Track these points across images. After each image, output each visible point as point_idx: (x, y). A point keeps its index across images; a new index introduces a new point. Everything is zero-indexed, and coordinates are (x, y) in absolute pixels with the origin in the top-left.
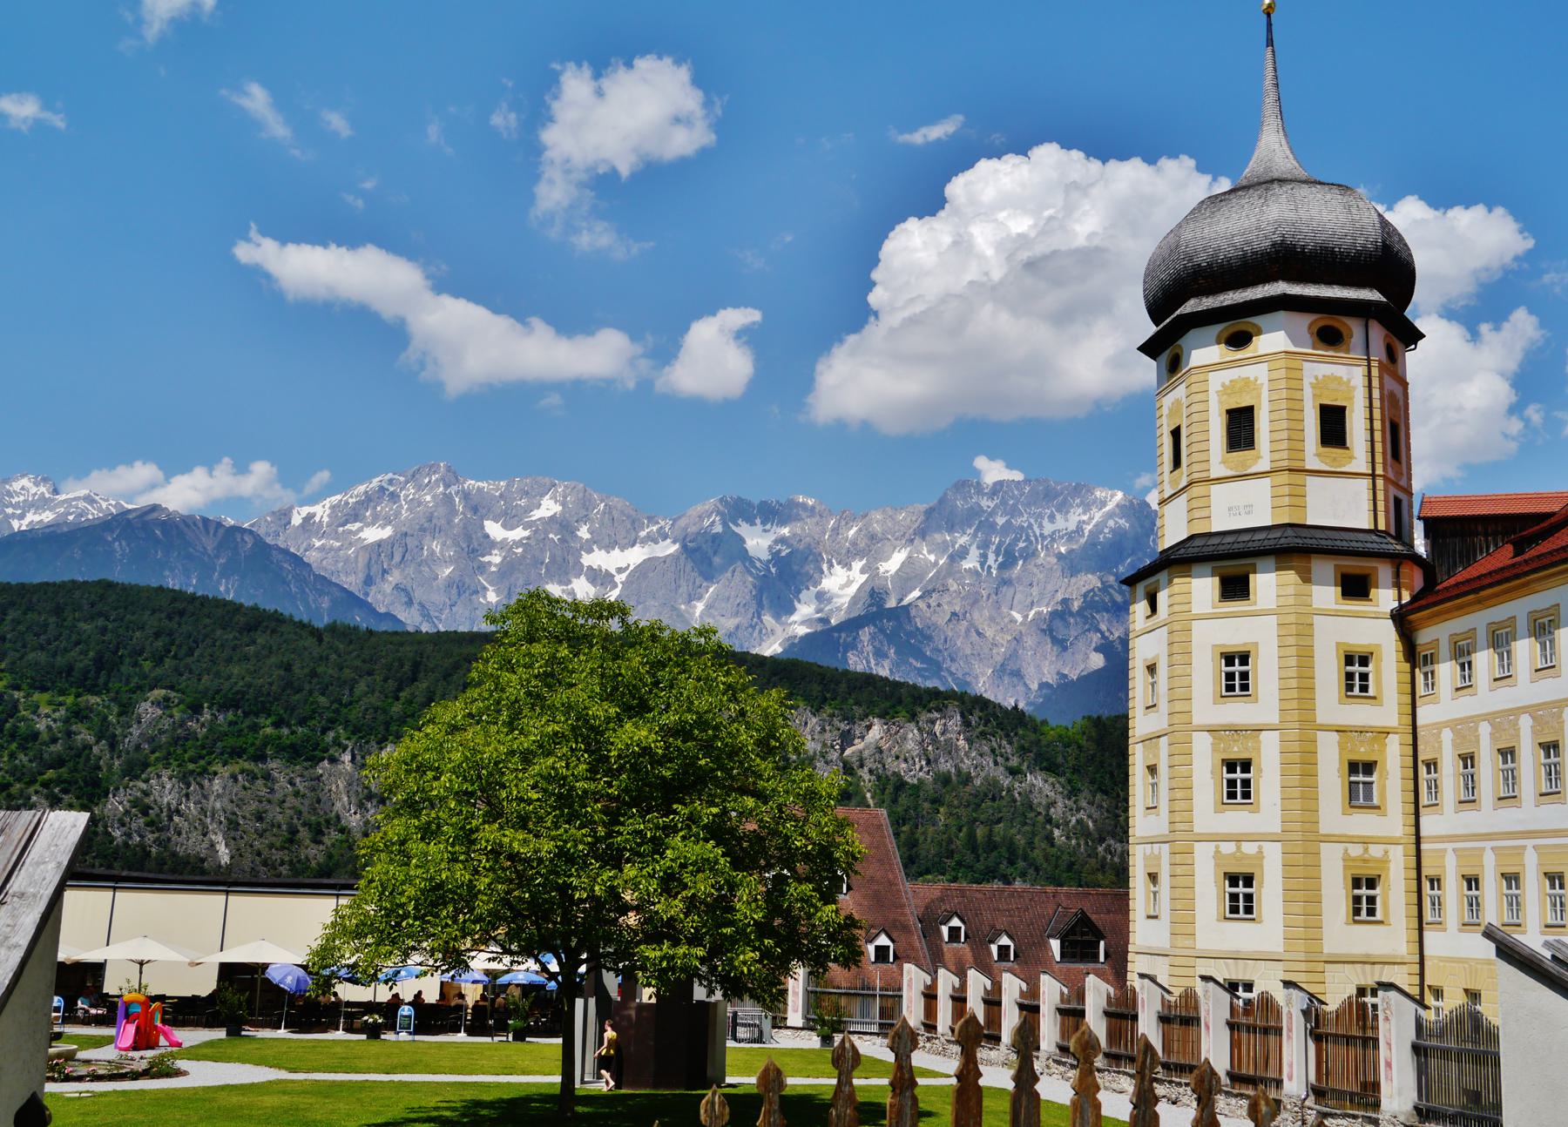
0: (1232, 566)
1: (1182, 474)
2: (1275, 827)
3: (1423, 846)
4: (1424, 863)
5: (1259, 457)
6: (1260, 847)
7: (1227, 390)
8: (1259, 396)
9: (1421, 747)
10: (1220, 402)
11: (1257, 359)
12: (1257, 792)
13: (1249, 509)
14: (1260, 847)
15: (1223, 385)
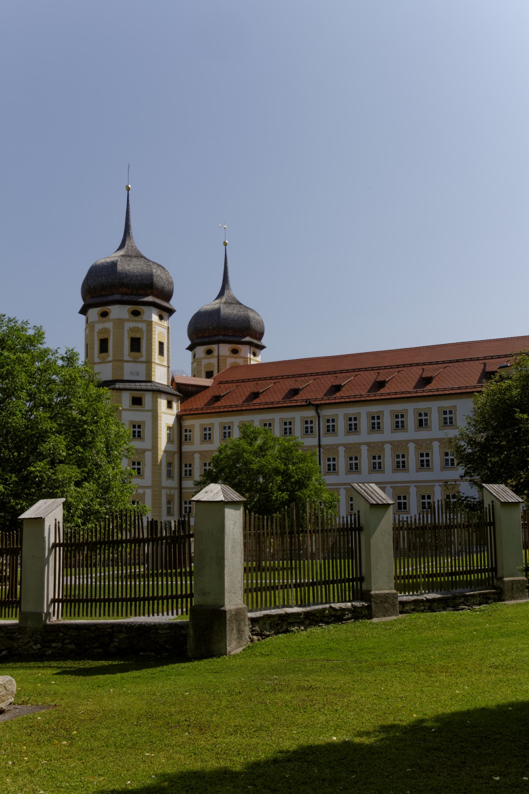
0: (137, 394)
1: (109, 356)
2: (149, 484)
3: (183, 491)
4: (183, 496)
5: (142, 356)
6: (144, 491)
7: (132, 330)
8: (143, 335)
9: (183, 459)
10: (128, 334)
11: (143, 321)
12: (144, 472)
13: (138, 374)
14: (144, 491)
15: (130, 328)
